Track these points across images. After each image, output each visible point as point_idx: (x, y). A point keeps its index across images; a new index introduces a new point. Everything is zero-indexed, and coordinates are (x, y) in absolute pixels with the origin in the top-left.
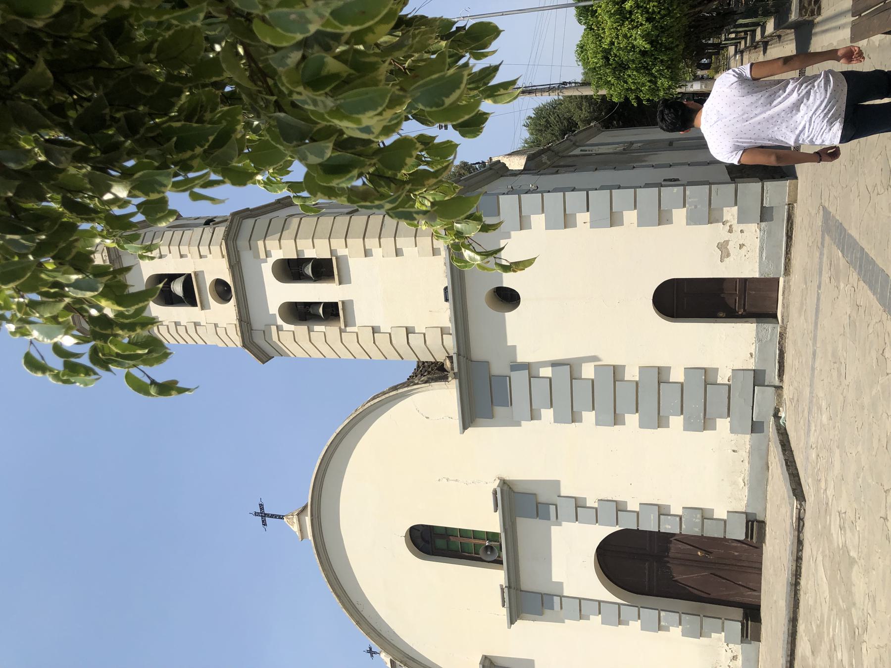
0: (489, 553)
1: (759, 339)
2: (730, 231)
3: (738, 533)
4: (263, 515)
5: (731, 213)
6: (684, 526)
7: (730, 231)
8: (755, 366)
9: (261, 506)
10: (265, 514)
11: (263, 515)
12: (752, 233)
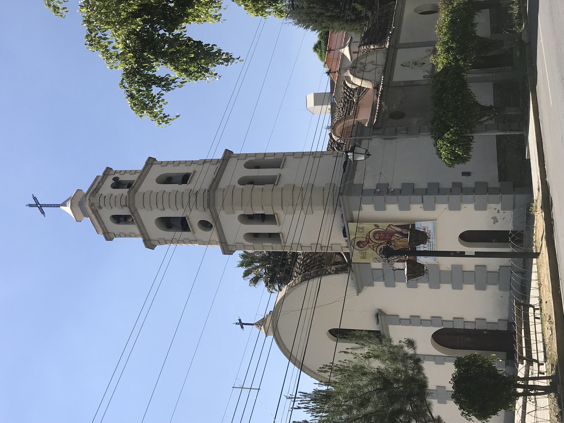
2: (498, 212)
3: (503, 327)
4: (241, 324)
5: (499, 206)
8: (514, 226)
9: (240, 320)
10: (242, 323)
11: (241, 324)
12: (509, 214)
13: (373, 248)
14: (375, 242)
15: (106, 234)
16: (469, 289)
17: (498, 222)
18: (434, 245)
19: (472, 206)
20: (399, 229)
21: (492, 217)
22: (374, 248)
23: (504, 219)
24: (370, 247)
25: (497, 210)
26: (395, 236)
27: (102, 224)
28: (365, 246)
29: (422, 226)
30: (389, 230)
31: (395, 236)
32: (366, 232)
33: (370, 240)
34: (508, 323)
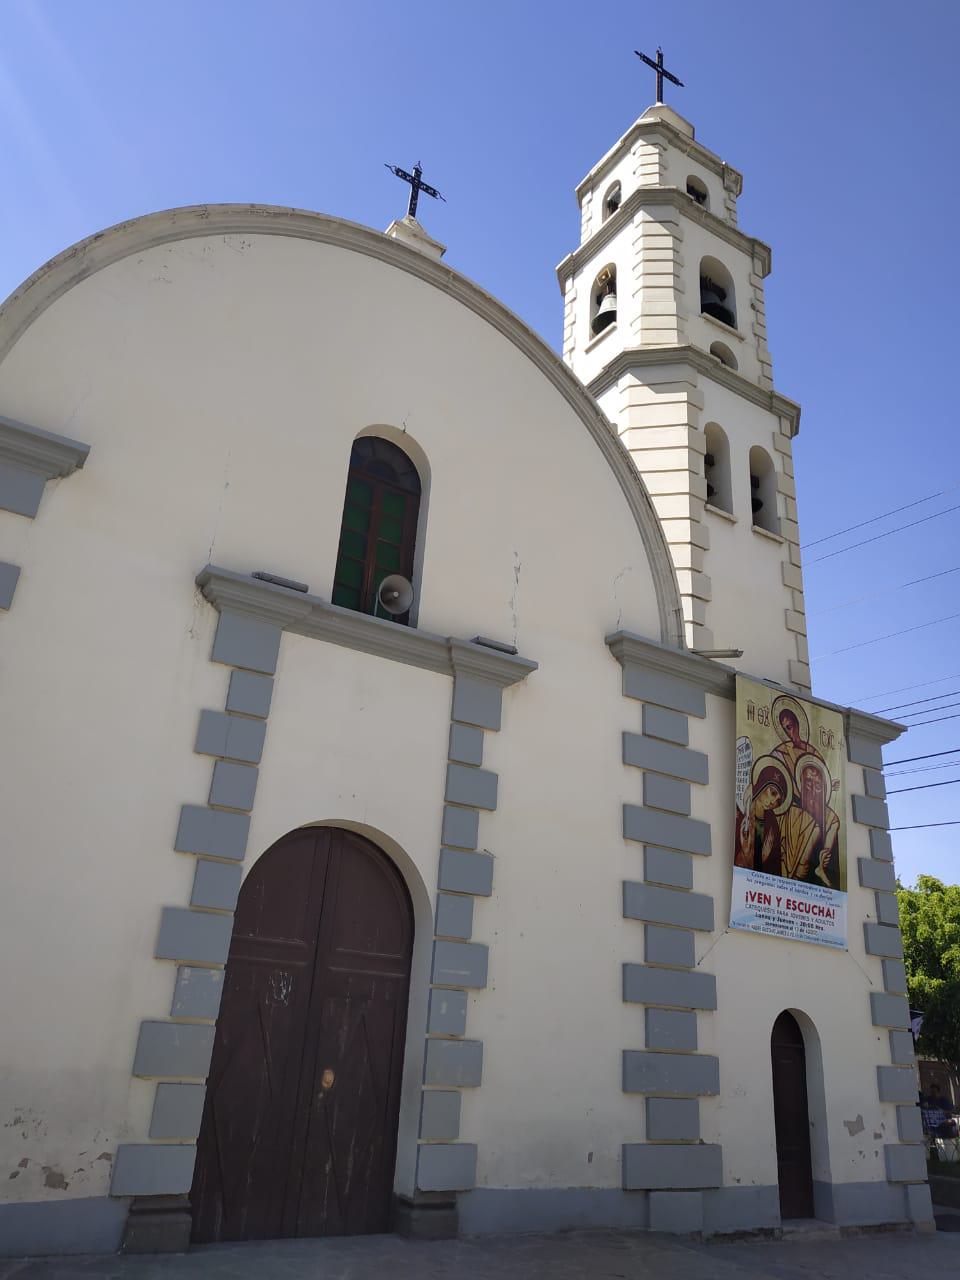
0: (396, 594)
1: (759, 1191)
2: (878, 1136)
6: (446, 1044)
7: (878, 1136)
13: (783, 753)
14: (798, 760)
15: (671, 136)
16: (628, 1028)
17: (852, 1134)
18: (782, 933)
19: (886, 1060)
20: (829, 843)
23: (861, 1152)
24: (785, 743)
25: (882, 1131)
26: (815, 826)
27: (693, 153)
28: (787, 733)
29: (836, 908)
31: (815, 826)
32: (820, 749)
34: (453, 1193)
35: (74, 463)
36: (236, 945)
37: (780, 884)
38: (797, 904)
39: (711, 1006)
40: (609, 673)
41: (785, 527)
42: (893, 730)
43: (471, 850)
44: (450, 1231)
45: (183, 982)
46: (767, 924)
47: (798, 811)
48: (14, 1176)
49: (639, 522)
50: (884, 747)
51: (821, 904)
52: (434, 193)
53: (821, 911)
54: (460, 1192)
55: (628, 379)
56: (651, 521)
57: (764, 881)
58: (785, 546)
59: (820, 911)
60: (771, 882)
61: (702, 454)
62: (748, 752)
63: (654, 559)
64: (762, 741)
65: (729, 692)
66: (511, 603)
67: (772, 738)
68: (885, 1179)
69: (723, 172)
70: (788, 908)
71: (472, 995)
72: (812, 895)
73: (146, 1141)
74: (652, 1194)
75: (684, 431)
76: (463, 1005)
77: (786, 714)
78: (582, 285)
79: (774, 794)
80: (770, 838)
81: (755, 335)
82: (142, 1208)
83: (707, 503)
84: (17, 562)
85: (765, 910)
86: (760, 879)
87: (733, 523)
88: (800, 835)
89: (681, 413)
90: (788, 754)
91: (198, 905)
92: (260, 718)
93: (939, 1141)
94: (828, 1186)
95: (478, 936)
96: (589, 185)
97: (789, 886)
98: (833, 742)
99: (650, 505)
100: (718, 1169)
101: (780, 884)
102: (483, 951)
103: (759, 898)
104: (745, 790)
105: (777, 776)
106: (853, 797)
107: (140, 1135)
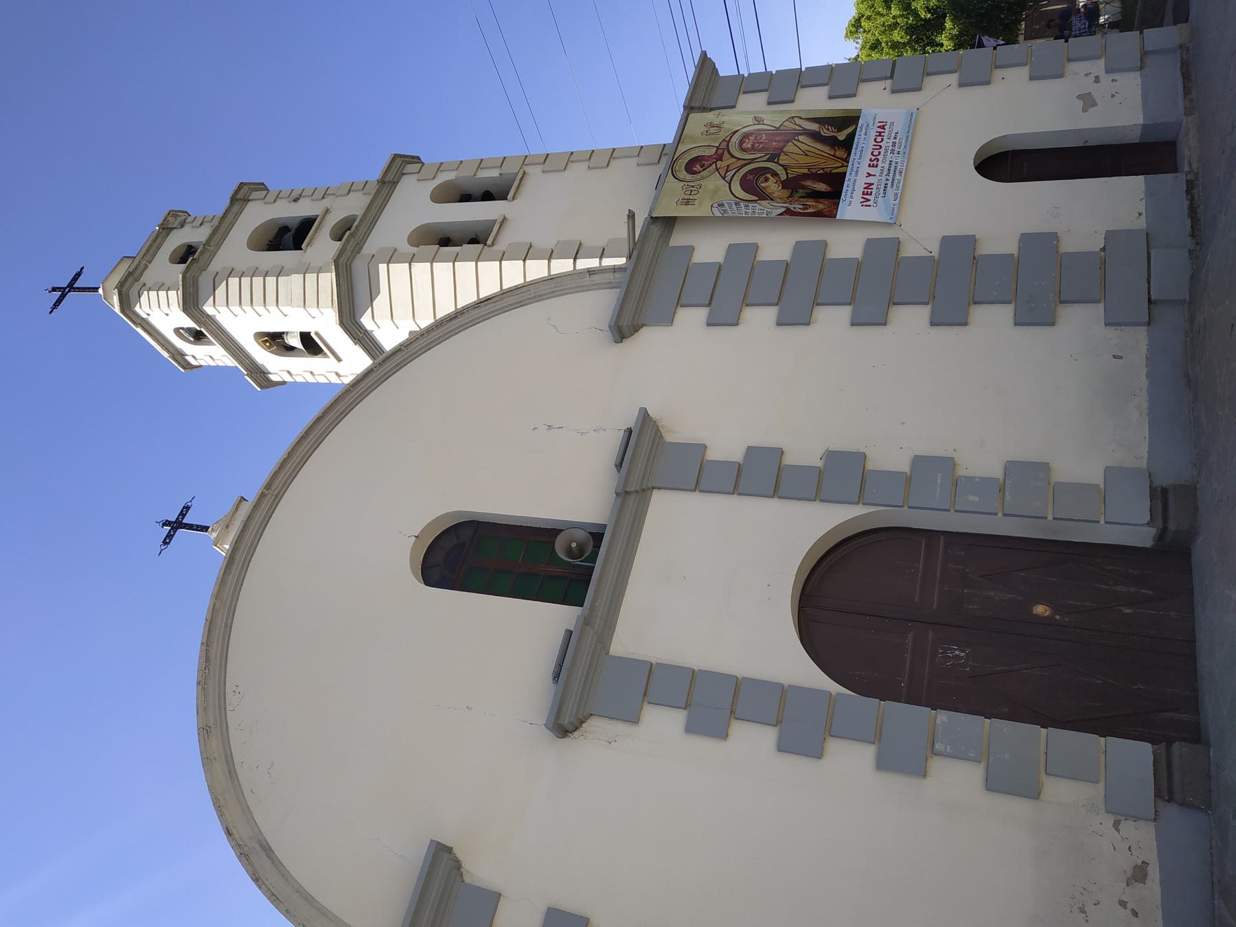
0: (574, 545)
1: (1150, 193)
2: (1097, 80)
5: (1098, 67)
6: (1008, 497)
7: (1097, 80)
13: (727, 171)
14: (733, 156)
15: (130, 279)
17: (1095, 104)
19: (1024, 71)
20: (814, 127)
21: (1079, 95)
22: (728, 174)
23: (1113, 96)
24: (717, 170)
26: (798, 141)
27: (147, 258)
28: (708, 167)
29: (877, 120)
30: (785, 128)
31: (798, 141)
32: (723, 135)
33: (726, 152)
34: (1153, 490)
35: (446, 856)
36: (912, 698)
37: (854, 173)
38: (873, 158)
39: (971, 241)
40: (650, 338)
41: (509, 169)
42: (705, 65)
43: (820, 473)
44: (1189, 492)
45: (948, 750)
46: (892, 185)
47: (782, 157)
48: (1135, 914)
49: (504, 310)
50: (721, 75)
51: (873, 134)
52: (187, 508)
53: (880, 134)
54: (1151, 482)
55: (366, 321)
56: (502, 299)
57: (850, 189)
58: (528, 169)
59: (880, 135)
60: (852, 181)
61: (439, 248)
62: (725, 204)
63: (540, 296)
64: (716, 192)
65: (669, 223)
66: (582, 434)
67: (712, 182)
68: (1138, 73)
69: (166, 229)
70: (877, 166)
71: (961, 471)
72: (864, 141)
73: (1101, 785)
74: (1153, 298)
75: (416, 266)
76: (970, 479)
77: (689, 168)
78: (276, 365)
79: (767, 180)
80: (809, 183)
81: (323, 198)
82: (1166, 790)
83: (486, 245)
84: (543, 910)
85: (877, 188)
86: (849, 193)
87: (505, 218)
88: (807, 155)
89: (399, 270)
90: (728, 166)
91: (876, 736)
92: (695, 676)
93: (1102, 20)
94: (1144, 125)
95: (905, 467)
96: (179, 358)
97: (856, 165)
98: (716, 122)
99: (488, 299)
100: (1129, 233)
101: (854, 173)
102: (918, 461)
103: (867, 194)
104: (762, 208)
105: (750, 177)
106: (769, 103)
107: (1095, 792)
